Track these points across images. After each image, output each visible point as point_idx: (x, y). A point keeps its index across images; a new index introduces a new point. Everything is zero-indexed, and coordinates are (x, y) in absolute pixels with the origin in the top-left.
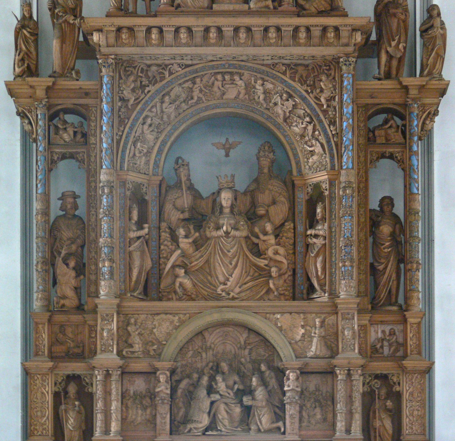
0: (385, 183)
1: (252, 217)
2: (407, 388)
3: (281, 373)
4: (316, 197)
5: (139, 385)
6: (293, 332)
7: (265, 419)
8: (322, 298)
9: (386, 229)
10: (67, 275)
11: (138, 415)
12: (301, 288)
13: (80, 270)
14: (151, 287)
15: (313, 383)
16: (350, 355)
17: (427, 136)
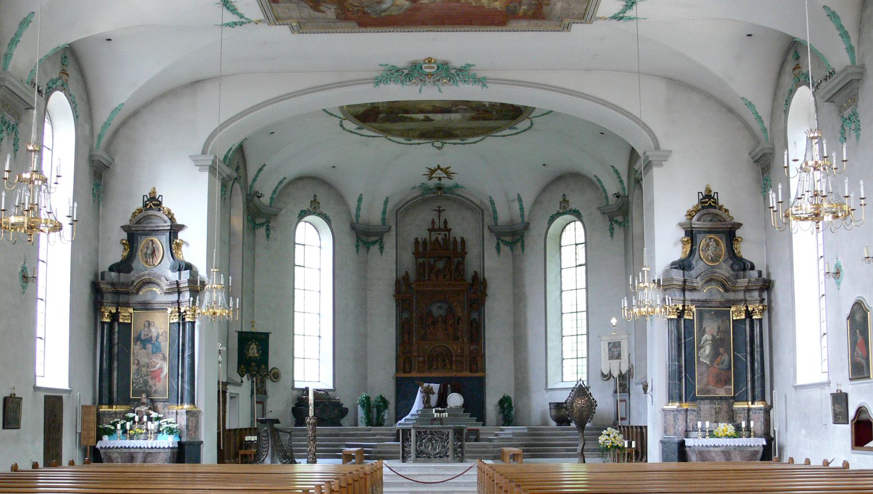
0: (475, 316)
1: (445, 323)
2: (478, 359)
3: (452, 356)
4: (459, 318)
5: (421, 359)
6: (454, 348)
7: (448, 366)
8: (461, 340)
9: (474, 325)
10: (406, 336)
11: (421, 365)
12: (456, 338)
13: (409, 334)
14: (423, 338)
15: (459, 358)
16: (466, 352)
17: (483, 305)
